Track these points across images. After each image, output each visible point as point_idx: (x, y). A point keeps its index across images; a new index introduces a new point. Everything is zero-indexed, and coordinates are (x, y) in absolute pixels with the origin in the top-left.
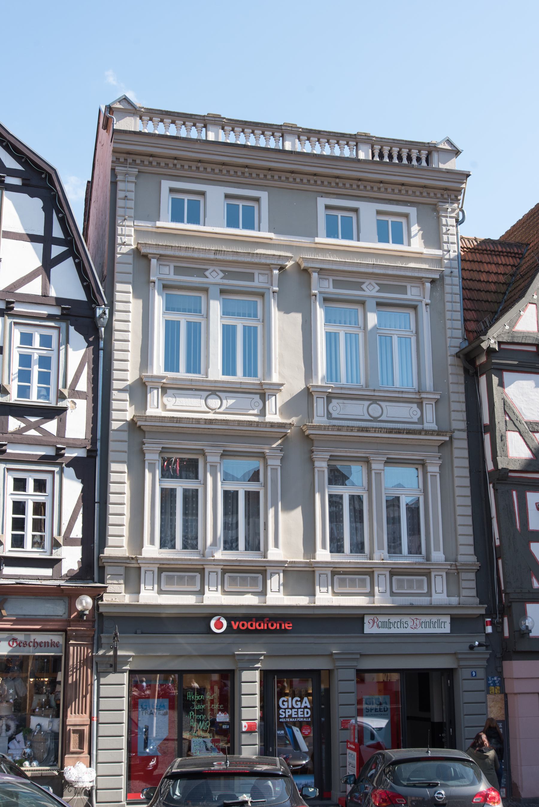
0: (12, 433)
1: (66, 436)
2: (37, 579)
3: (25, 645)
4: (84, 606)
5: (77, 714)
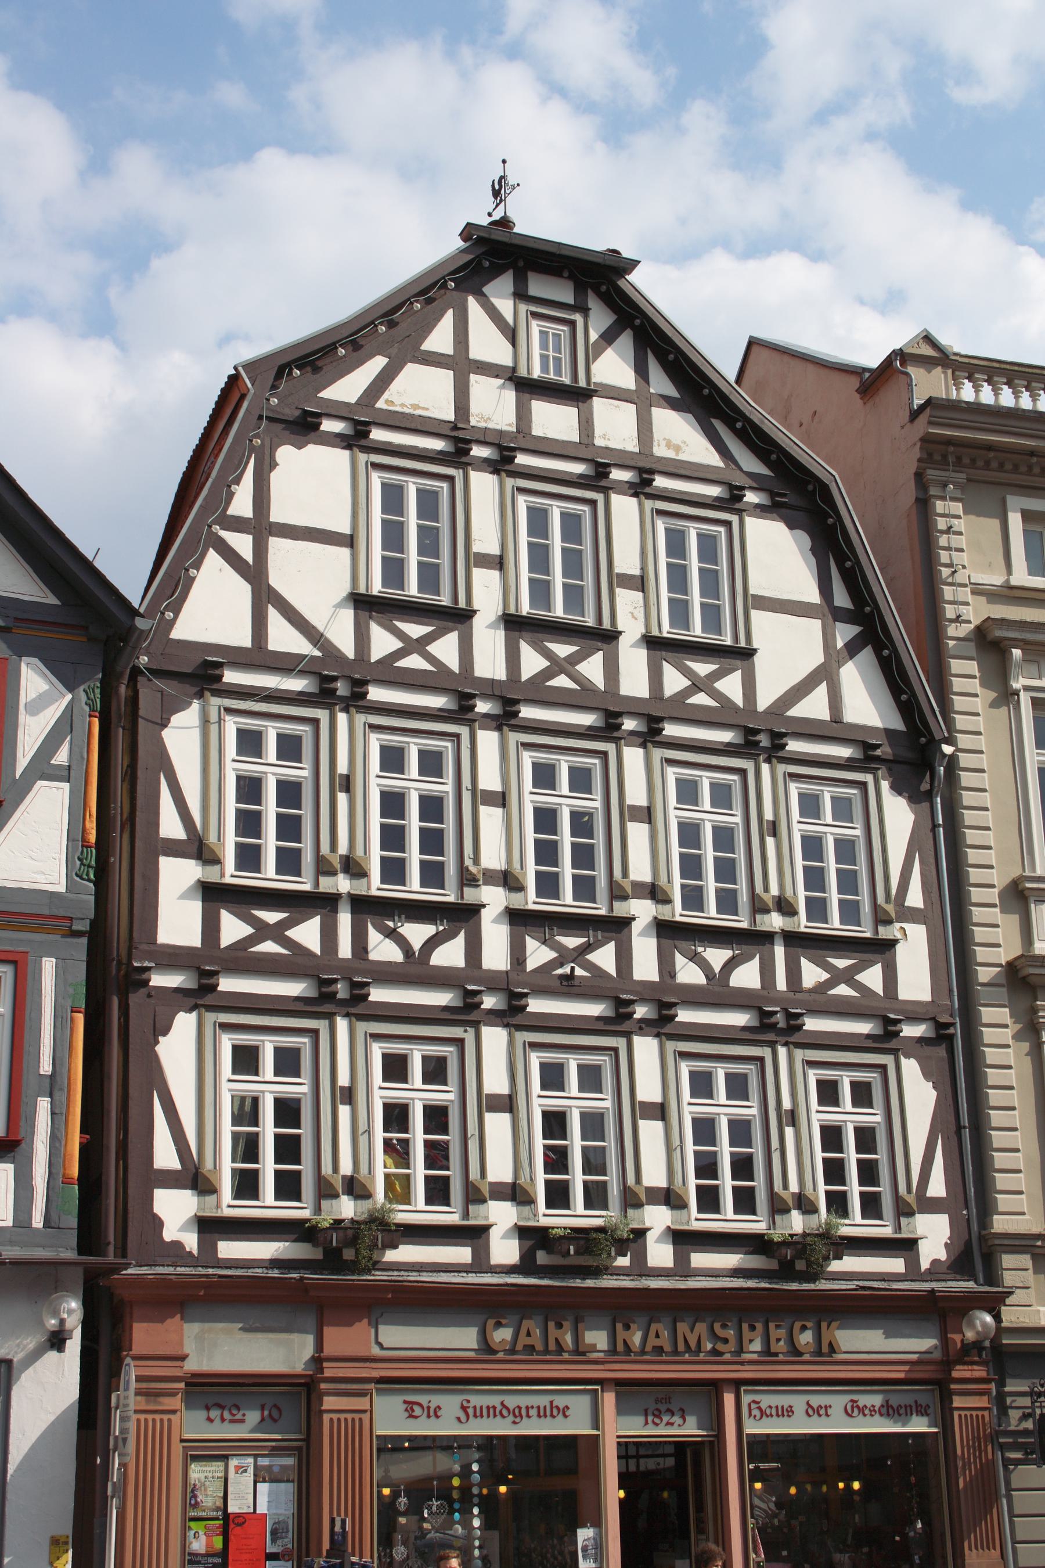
0: (810, 991)
1: (900, 997)
2: (881, 1280)
3: (873, 1413)
4: (978, 1333)
5: (993, 1551)
